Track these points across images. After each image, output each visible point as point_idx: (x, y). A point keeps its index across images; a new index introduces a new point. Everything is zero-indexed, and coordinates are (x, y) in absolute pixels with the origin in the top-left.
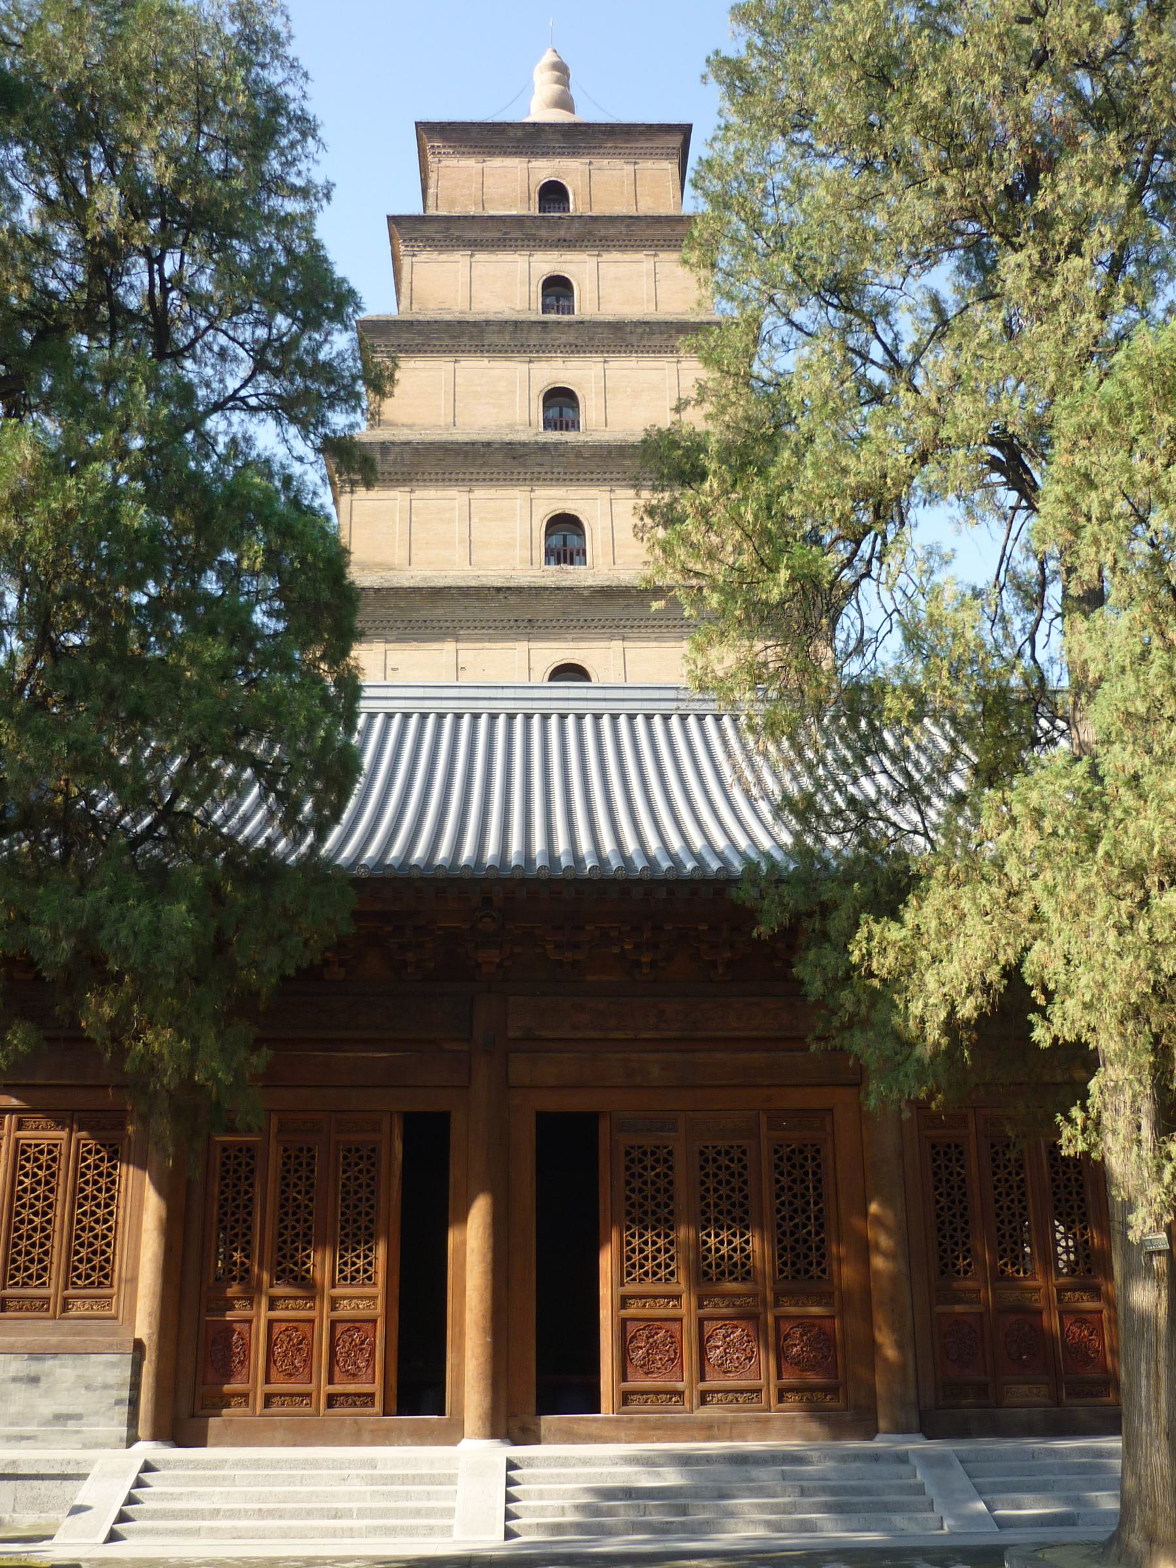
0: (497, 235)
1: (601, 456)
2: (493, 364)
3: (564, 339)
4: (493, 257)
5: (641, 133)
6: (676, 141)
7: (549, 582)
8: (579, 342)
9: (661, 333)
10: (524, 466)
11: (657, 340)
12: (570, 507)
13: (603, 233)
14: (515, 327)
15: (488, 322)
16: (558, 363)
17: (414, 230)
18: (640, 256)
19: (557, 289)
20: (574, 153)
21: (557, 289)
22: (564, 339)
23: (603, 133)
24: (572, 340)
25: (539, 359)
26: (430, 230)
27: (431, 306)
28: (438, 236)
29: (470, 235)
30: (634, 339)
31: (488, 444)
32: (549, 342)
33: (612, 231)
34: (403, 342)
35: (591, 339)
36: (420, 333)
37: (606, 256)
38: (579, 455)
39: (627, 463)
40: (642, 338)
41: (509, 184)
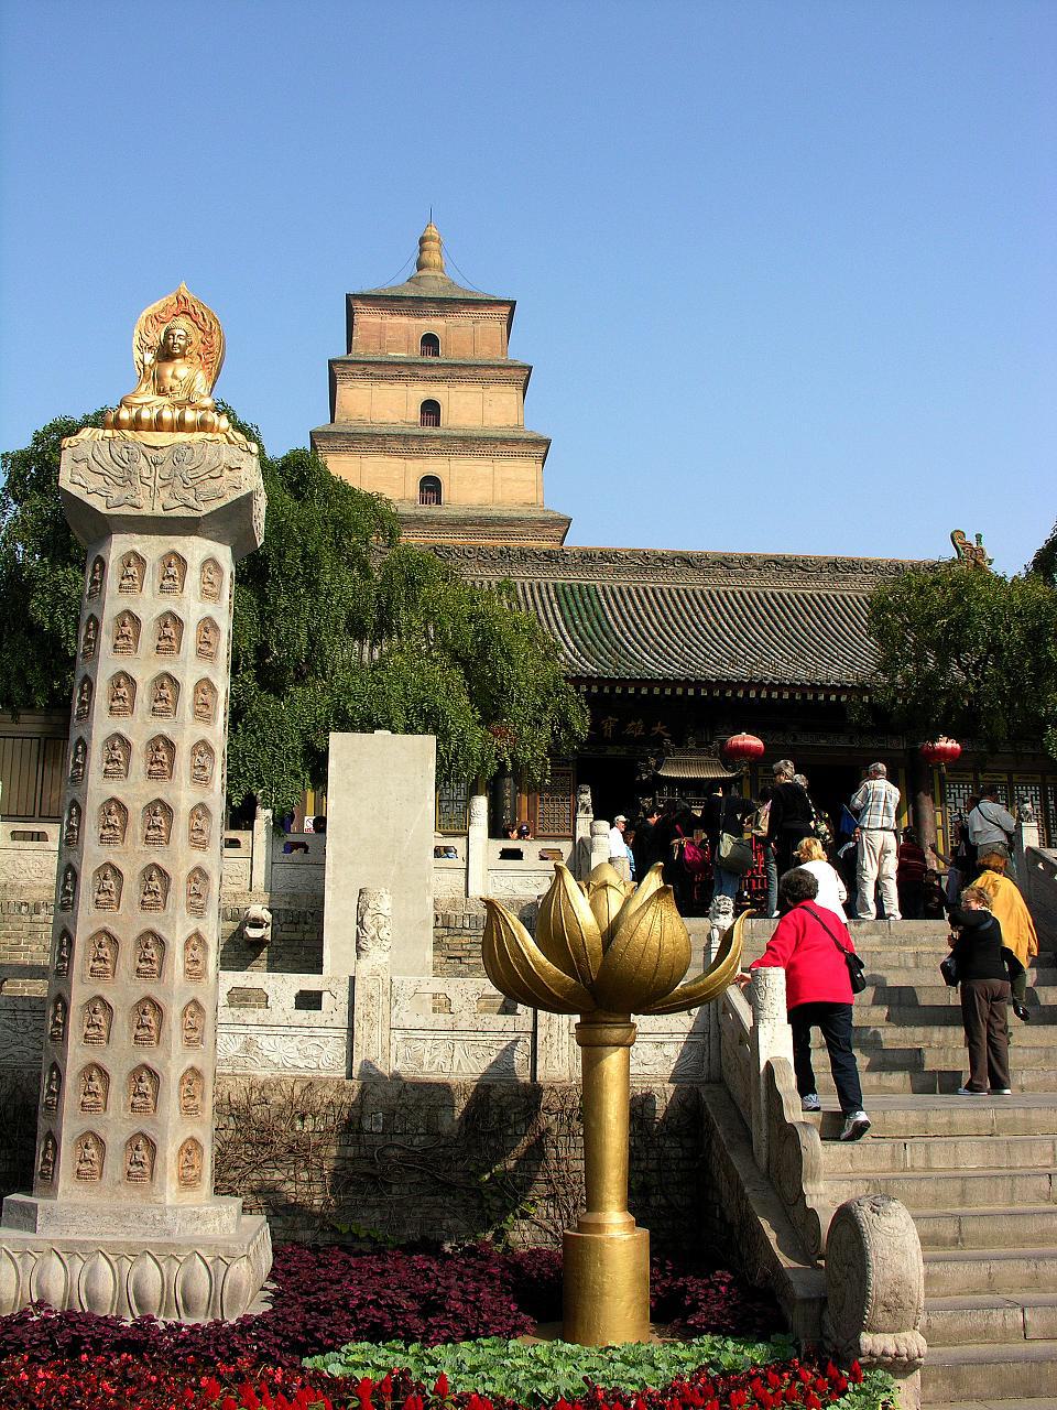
5: (485, 304)
11: (489, 448)
14: (405, 438)
16: (430, 461)
17: (345, 369)
21: (431, 409)
25: (418, 458)
28: (359, 373)
33: (465, 373)
37: (458, 388)
39: (468, 528)
41: (399, 333)
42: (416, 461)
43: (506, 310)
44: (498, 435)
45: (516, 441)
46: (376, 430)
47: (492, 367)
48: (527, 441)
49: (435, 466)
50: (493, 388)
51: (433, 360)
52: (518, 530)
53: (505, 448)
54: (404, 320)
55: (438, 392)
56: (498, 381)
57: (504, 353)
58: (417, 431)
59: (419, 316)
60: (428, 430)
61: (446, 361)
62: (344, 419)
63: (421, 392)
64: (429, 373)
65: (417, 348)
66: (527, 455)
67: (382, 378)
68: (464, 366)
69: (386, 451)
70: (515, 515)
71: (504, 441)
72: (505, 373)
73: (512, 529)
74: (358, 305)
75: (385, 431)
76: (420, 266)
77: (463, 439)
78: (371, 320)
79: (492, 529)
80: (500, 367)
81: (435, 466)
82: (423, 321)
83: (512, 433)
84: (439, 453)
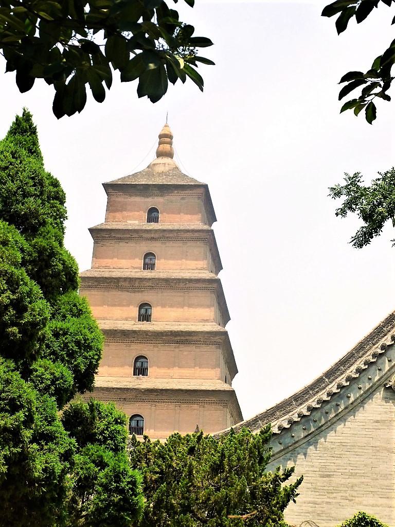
0: (129, 236)
3: (148, 284)
6: (202, 190)
7: (130, 386)
9: (183, 282)
11: (182, 285)
12: (143, 353)
14: (131, 280)
18: (180, 244)
19: (149, 262)
20: (162, 196)
22: (148, 284)
23: (173, 187)
24: (150, 285)
25: (139, 292)
26: (104, 234)
29: (119, 236)
30: (172, 284)
31: (116, 330)
32: (143, 285)
33: (171, 235)
36: (96, 281)
37: (167, 244)
38: (147, 335)
40: (176, 284)
42: (137, 294)
43: (202, 190)
47: (188, 231)
49: (147, 297)
50: (189, 244)
52: (194, 338)
53: (192, 285)
58: (138, 275)
59: (147, 197)
60: (148, 274)
64: (149, 236)
66: (206, 289)
67: (120, 239)
72: (196, 234)
73: (191, 338)
82: (150, 200)
83: (196, 275)
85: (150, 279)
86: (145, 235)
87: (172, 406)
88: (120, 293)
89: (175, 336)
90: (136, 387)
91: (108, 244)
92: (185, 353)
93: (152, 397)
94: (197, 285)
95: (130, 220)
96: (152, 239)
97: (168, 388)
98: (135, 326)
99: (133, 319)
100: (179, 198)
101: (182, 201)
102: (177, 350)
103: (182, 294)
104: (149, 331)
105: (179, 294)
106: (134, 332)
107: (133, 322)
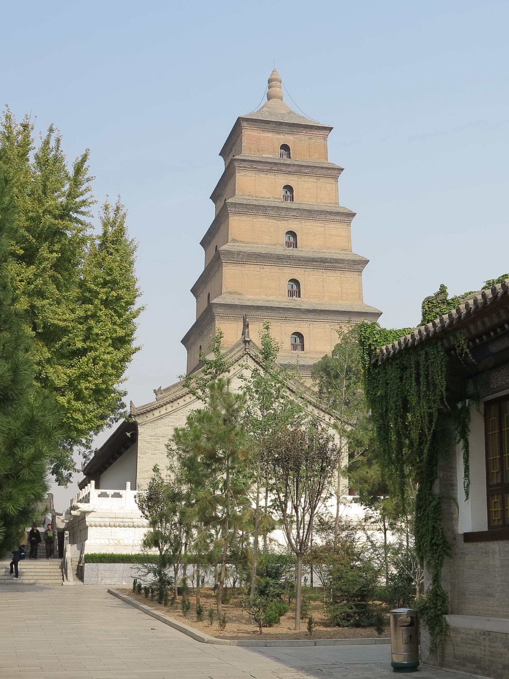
0: (269, 168)
1: (306, 261)
2: (269, 221)
3: (293, 214)
4: (267, 176)
5: (316, 129)
7: (291, 305)
8: (297, 215)
10: (282, 262)
11: (323, 217)
13: (304, 171)
15: (269, 207)
22: (293, 214)
27: (246, 194)
28: (249, 166)
29: (258, 167)
34: (240, 210)
35: (301, 215)
37: (303, 179)
39: (314, 263)
42: (283, 222)
44: (328, 209)
45: (337, 214)
46: (261, 203)
47: (322, 168)
48: (343, 214)
49: (294, 225)
50: (322, 180)
51: (288, 162)
52: (341, 265)
54: (270, 135)
55: (292, 180)
56: (325, 176)
57: (327, 159)
59: (279, 133)
60: (288, 204)
61: (296, 163)
62: (241, 194)
63: (283, 180)
65: (278, 153)
68: (307, 167)
69: (266, 215)
70: (340, 257)
71: (331, 213)
72: (329, 171)
73: (337, 265)
74: (244, 124)
75: (266, 204)
76: (269, 97)
77: (310, 211)
78: (251, 133)
79: (327, 264)
80: (326, 168)
81: (294, 225)
82: (281, 136)
83: (334, 208)
84: (295, 217)
85: (295, 209)
86: (284, 169)
87: (327, 325)
88: (267, 220)
89: (325, 262)
90: (298, 307)
91: (249, 174)
92: (332, 278)
93: (311, 316)
94: (337, 218)
95: (264, 154)
96: (290, 173)
97: (326, 309)
98: (286, 252)
99: (281, 245)
100: (307, 138)
101: (310, 141)
102: (325, 275)
103: (323, 225)
104: (302, 257)
105: (320, 225)
106: (289, 257)
107: (281, 248)
